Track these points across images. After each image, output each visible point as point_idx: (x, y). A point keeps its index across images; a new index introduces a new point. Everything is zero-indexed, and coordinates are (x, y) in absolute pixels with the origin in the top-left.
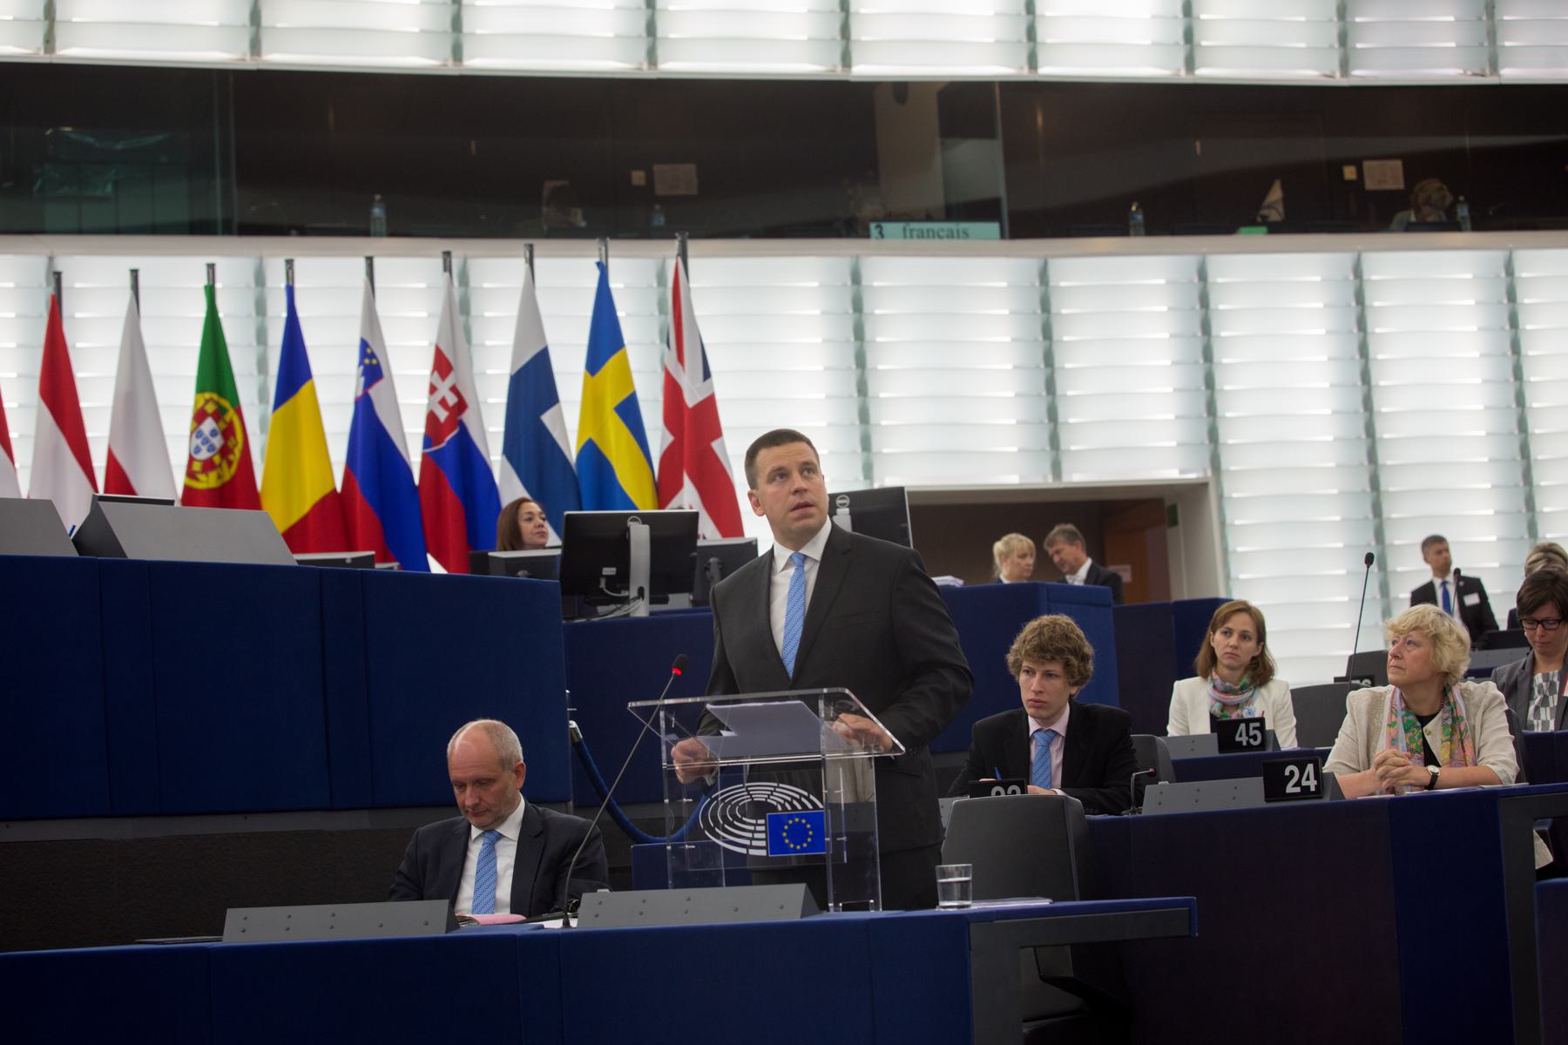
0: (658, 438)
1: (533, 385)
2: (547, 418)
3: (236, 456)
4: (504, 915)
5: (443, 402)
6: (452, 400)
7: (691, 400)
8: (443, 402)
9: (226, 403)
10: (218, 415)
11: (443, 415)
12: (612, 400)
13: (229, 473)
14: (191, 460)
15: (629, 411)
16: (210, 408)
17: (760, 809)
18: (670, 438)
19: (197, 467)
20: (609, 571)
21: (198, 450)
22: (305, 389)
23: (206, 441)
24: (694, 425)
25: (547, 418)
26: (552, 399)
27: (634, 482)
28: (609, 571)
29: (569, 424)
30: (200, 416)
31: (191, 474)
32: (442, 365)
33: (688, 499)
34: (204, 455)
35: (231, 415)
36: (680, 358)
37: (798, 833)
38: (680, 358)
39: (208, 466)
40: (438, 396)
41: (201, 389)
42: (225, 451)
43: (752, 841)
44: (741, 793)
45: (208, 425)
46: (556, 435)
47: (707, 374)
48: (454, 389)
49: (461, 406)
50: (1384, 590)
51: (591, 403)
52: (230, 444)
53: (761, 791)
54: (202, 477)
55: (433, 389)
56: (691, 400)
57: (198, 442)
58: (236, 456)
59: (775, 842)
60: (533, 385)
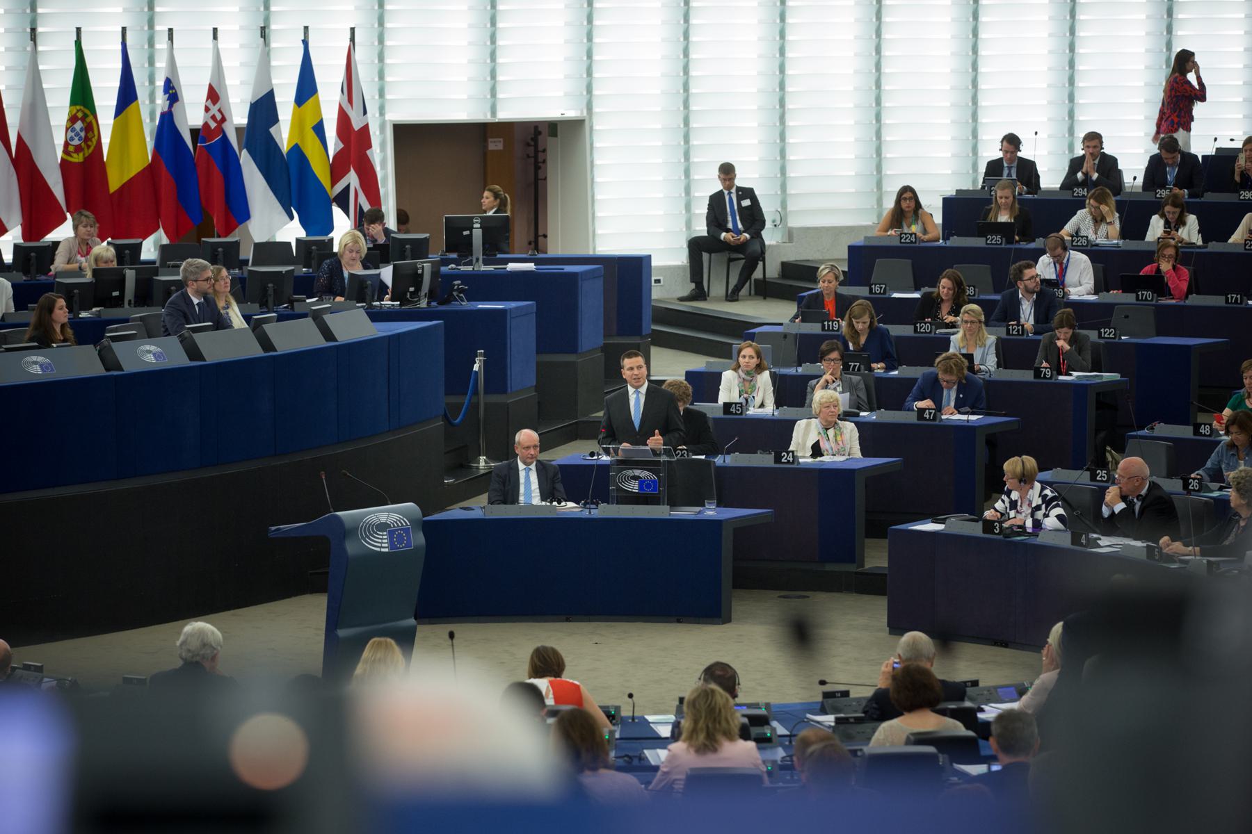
0: (333, 144)
1: (264, 109)
2: (273, 130)
3: (94, 140)
4: (536, 500)
5: (213, 117)
6: (219, 117)
7: (357, 125)
8: (213, 117)
9: (87, 111)
10: (83, 119)
11: (213, 125)
12: (310, 123)
13: (87, 152)
14: (66, 144)
15: (319, 129)
16: (80, 115)
17: (635, 478)
18: (341, 146)
19: (71, 149)
20: (412, 289)
21: (72, 139)
22: (133, 105)
23: (77, 134)
24: (355, 141)
25: (273, 130)
26: (274, 119)
27: (321, 171)
28: (412, 289)
29: (284, 134)
30: (73, 119)
31: (66, 151)
32: (213, 95)
33: (352, 179)
34: (76, 142)
35: (91, 118)
36: (350, 100)
37: (648, 486)
38: (350, 100)
39: (78, 149)
40: (211, 113)
41: (73, 103)
42: (87, 139)
43: (634, 487)
44: (630, 473)
45: (79, 125)
46: (277, 140)
47: (365, 112)
48: (219, 110)
49: (223, 119)
50: (688, 190)
51: (298, 123)
52: (90, 135)
53: (637, 472)
54: (75, 155)
55: (207, 109)
56: (357, 125)
57: (70, 134)
58: (94, 140)
59: (641, 487)
60: (264, 109)
